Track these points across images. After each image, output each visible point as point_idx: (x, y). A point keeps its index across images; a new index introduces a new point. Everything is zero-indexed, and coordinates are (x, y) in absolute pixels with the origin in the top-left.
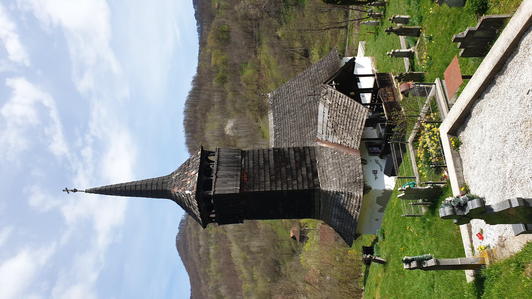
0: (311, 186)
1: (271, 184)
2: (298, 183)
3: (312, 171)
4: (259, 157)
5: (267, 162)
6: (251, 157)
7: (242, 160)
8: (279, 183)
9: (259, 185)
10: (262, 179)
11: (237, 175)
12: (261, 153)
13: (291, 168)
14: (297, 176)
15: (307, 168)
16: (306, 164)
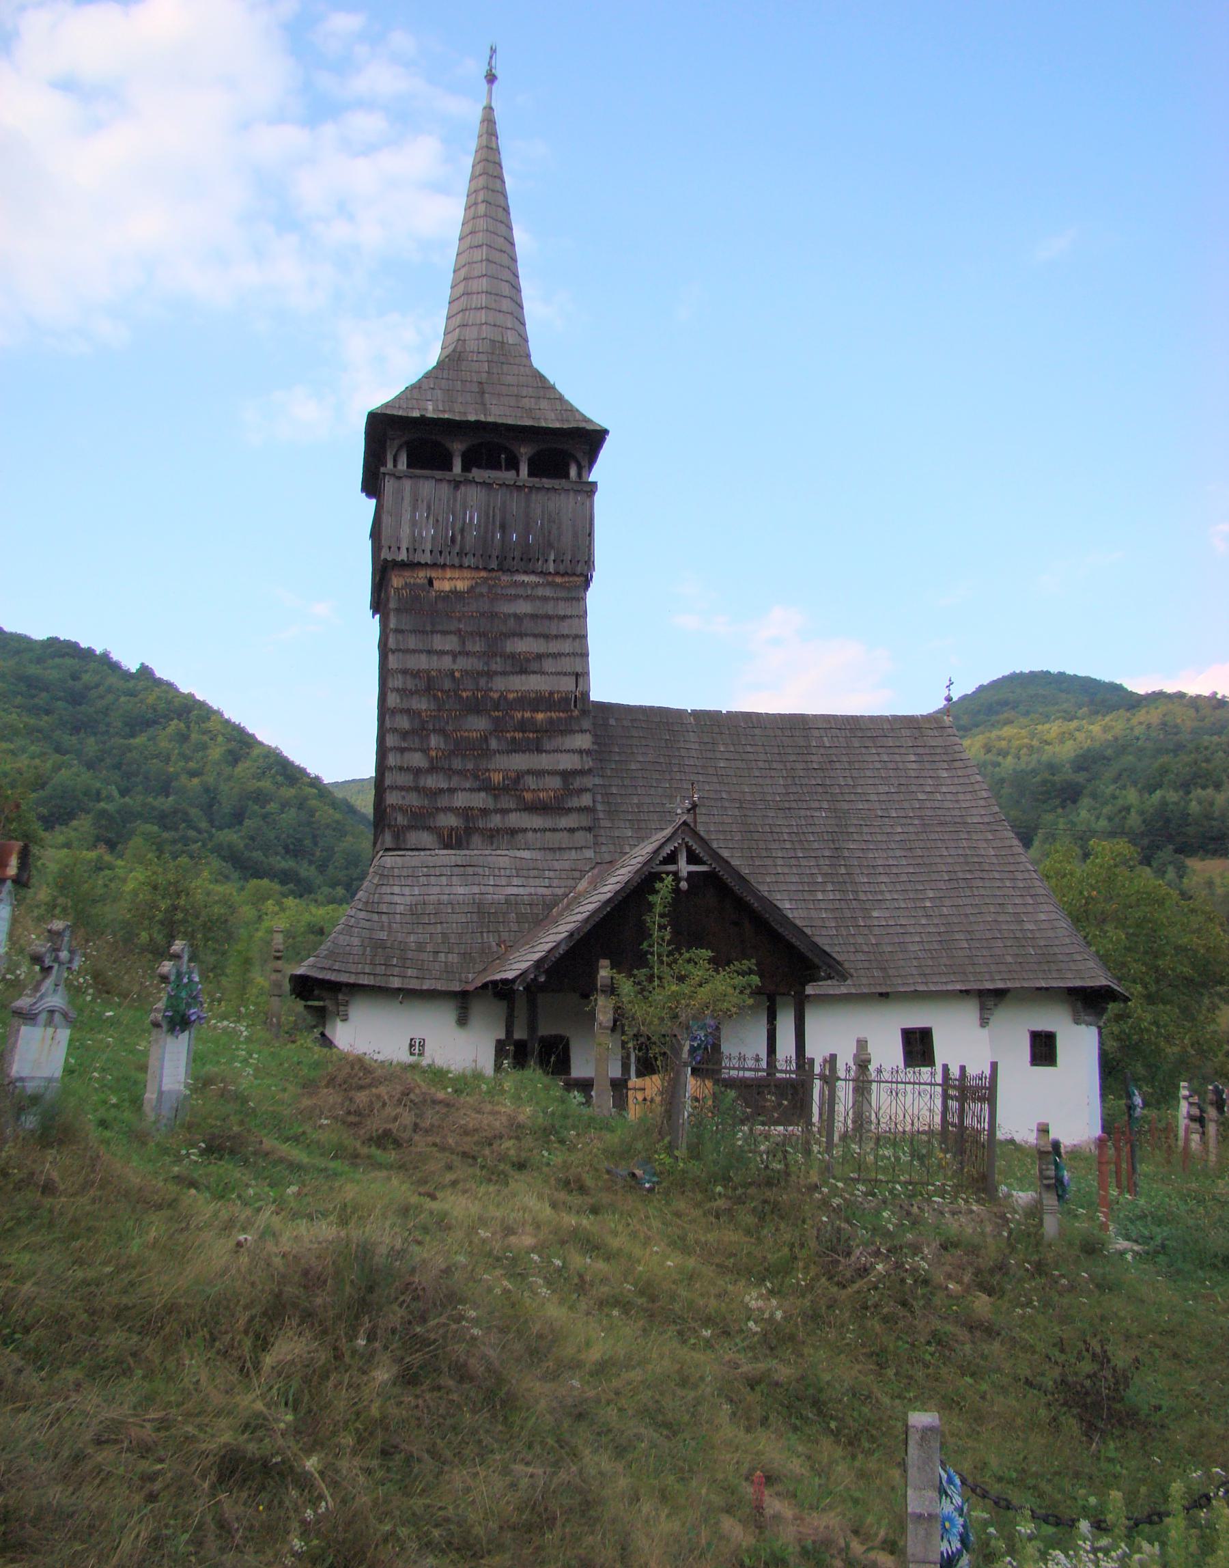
0: (401, 820)
1: (416, 674)
2: (417, 772)
3: (469, 831)
4: (546, 637)
5: (522, 665)
6: (549, 609)
7: (533, 572)
8: (421, 704)
9: (414, 631)
10: (451, 643)
11: (462, 554)
12: (566, 647)
13: (487, 753)
14: (450, 772)
15: (485, 812)
16: (504, 812)
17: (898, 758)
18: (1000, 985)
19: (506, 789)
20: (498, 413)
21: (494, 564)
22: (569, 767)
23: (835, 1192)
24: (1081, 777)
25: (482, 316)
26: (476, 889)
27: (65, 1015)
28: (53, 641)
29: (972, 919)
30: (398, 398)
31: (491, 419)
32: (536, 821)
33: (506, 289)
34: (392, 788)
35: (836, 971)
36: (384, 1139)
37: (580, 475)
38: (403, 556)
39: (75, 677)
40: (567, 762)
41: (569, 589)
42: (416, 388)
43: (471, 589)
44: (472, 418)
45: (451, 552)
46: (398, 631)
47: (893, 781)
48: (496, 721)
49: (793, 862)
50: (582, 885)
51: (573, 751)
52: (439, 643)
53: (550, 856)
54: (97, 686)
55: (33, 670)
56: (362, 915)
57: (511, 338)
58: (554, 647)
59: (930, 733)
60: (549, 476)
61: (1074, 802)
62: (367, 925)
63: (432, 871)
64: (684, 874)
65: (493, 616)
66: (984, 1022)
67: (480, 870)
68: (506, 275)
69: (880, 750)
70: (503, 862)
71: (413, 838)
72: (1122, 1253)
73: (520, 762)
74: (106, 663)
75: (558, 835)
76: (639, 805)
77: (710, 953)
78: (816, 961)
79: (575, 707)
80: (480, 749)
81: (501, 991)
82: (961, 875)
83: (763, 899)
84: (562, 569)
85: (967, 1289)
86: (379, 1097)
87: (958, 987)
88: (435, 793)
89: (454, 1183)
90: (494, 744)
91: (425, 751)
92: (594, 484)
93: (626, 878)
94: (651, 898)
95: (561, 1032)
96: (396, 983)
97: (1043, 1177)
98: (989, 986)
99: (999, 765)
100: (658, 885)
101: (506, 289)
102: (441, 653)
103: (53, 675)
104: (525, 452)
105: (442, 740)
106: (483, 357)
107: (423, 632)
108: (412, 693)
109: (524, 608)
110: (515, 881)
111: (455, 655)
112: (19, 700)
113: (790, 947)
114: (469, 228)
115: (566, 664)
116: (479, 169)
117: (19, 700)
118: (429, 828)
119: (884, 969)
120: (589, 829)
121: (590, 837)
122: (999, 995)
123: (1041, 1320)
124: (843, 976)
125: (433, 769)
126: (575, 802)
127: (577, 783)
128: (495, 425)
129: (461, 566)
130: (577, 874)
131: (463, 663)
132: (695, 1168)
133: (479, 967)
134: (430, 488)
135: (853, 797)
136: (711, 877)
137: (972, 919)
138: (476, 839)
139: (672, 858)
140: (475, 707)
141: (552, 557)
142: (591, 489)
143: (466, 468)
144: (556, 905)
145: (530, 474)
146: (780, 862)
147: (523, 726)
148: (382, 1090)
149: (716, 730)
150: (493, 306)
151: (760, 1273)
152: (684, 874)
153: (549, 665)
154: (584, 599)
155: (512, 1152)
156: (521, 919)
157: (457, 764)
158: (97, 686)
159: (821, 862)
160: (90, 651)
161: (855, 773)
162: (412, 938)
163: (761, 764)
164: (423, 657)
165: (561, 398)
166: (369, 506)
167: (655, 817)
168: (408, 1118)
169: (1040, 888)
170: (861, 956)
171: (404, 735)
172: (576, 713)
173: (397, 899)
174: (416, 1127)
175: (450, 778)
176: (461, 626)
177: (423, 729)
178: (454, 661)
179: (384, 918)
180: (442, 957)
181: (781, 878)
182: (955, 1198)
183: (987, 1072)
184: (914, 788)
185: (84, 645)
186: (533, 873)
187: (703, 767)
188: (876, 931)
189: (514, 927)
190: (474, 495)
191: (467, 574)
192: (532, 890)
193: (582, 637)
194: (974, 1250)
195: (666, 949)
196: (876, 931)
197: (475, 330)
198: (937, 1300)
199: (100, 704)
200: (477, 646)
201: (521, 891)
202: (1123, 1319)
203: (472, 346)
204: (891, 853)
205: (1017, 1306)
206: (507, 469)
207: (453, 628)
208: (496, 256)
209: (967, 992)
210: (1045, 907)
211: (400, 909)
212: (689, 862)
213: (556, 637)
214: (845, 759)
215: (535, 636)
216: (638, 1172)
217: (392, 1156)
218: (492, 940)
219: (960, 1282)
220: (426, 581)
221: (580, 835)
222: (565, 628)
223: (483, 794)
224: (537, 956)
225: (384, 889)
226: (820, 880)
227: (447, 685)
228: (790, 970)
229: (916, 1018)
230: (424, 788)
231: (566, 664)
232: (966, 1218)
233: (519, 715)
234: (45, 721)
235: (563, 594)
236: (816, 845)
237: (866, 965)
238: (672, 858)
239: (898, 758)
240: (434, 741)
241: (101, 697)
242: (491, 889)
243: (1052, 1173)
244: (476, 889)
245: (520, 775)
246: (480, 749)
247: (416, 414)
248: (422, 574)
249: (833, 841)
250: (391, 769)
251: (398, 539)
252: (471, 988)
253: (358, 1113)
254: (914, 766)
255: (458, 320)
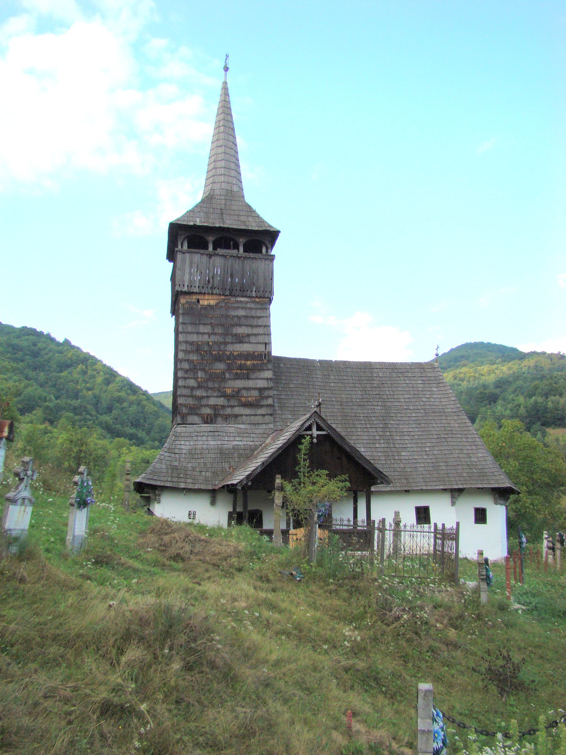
0: (185, 410)
1: (192, 343)
2: (192, 388)
3: (216, 416)
4: (252, 326)
5: (240, 339)
6: (253, 313)
7: (246, 296)
8: (194, 357)
9: (191, 324)
10: (208, 329)
12: (261, 331)
13: (224, 380)
14: (207, 389)
15: (223, 407)
16: (232, 407)
17: (413, 382)
18: (461, 487)
19: (233, 396)
20: (230, 223)
21: (227, 293)
22: (262, 386)
23: (384, 582)
24: (498, 391)
25: (222, 179)
26: (219, 443)
27: (30, 500)
28: (24, 329)
29: (448, 456)
30: (183, 216)
31: (226, 226)
32: (247, 411)
33: (233, 166)
34: (180, 396)
35: (385, 480)
36: (177, 558)
37: (267, 252)
38: (186, 289)
39: (35, 345)
40: (261, 384)
41: (262, 304)
42: (192, 211)
43: (217, 304)
44: (217, 225)
45: (208, 287)
46: (183, 323)
47: (411, 392)
48: (229, 365)
49: (365, 430)
50: (268, 441)
51: (264, 379)
52: (202, 329)
53: (253, 427)
54: (45, 349)
55: (15, 341)
56: (167, 454)
57: (235, 189)
58: (255, 331)
59: (429, 370)
60: (253, 252)
61: (495, 402)
62: (169, 459)
63: (199, 434)
64: (315, 435)
65: (227, 316)
66: (453, 504)
67: (221, 434)
68: (233, 160)
69: (405, 378)
70: (232, 430)
71: (190, 419)
72: (517, 610)
73: (240, 384)
74: (49, 338)
75: (257, 417)
76: (294, 404)
77: (327, 472)
78: (376, 475)
79: (265, 359)
80: (221, 378)
81: (231, 489)
82: (443, 436)
83: (351, 447)
84: (259, 295)
85: (446, 627)
86: (174, 538)
87: (441, 487)
88: (201, 398)
89: (209, 578)
90: (227, 375)
91: (196, 379)
92: (274, 256)
93: (288, 437)
94: (300, 446)
95: (258, 508)
96: (182, 486)
97: (480, 575)
98: (456, 487)
99: (460, 385)
100: (303, 441)
101: (233, 166)
102: (203, 334)
103: (24, 344)
104: (242, 241)
105: (203, 374)
106: (223, 197)
107: (195, 324)
108: (190, 352)
109: (241, 313)
110: (237, 439)
111: (209, 335)
112: (9, 355)
113: (364, 468)
114: (216, 138)
115: (261, 339)
116: (221, 111)
117: (9, 355)
118: (197, 414)
119: (407, 479)
120: (271, 415)
121: (271, 418)
122: (460, 491)
123: (479, 641)
124: (388, 482)
125: (199, 387)
126: (265, 402)
127: (266, 393)
128: (228, 228)
129: (212, 294)
130: (266, 436)
131: (213, 338)
132: (320, 571)
133: (221, 478)
134: (198, 258)
135: (393, 400)
136: (328, 436)
137: (448, 456)
138: (219, 419)
139: (309, 428)
140: (219, 359)
141: (254, 290)
142: (272, 258)
143: (215, 248)
144: (256, 449)
145: (244, 251)
146: (359, 430)
147: (241, 367)
148: (176, 535)
149: (330, 369)
150: (227, 173)
151: (350, 619)
152: (315, 435)
153: (253, 339)
154: (269, 309)
155: (236, 564)
156: (240, 456)
157: (210, 384)
158: (45, 349)
159: (378, 430)
160: (41, 334)
161: (394, 389)
162: (190, 465)
163: (350, 385)
164: (195, 336)
165: (258, 216)
166: (170, 266)
167: (302, 409)
168: (188, 548)
169: (479, 442)
170: (396, 473)
171: (186, 371)
172: (265, 361)
173: (183, 447)
174: (192, 552)
175: (207, 391)
176: (213, 321)
177: (195, 369)
178: (209, 337)
179: (177, 456)
180: (203, 474)
181: (360, 437)
182: (440, 584)
183: (455, 527)
184: (421, 396)
185: (39, 330)
186: (245, 435)
187: (324, 386)
188: (404, 461)
189: (237, 460)
190: (218, 261)
191: (215, 297)
192: (245, 443)
193: (268, 326)
194: (449, 608)
195: (307, 470)
196: (404, 461)
197: (219, 184)
198: (431, 632)
199: (46, 357)
200: (220, 330)
201: (240, 443)
202: (517, 640)
203: (217, 192)
204: (410, 426)
205: (468, 634)
206: (234, 249)
207: (209, 322)
208: (228, 151)
209: (445, 490)
210: (481, 451)
211: (184, 451)
212: (317, 430)
213: (256, 326)
214: (389, 382)
215: (246, 326)
216: (294, 573)
217: (181, 565)
218: (226, 466)
219: (442, 623)
220: (196, 301)
221: (267, 417)
222: (260, 322)
223: (222, 399)
224: (247, 473)
225: (177, 442)
226: (378, 438)
227: (206, 348)
228: (364, 479)
229: (422, 502)
230: (195, 396)
231: (261, 339)
232: (445, 594)
233: (239, 362)
234: (21, 365)
235: (259, 306)
236: (376, 422)
237: (399, 477)
238: (309, 428)
239: (413, 382)
240: (200, 374)
241: (47, 354)
242: (226, 442)
243: (484, 573)
244: (219, 443)
245: (239, 390)
246: (221, 378)
247: (192, 224)
248: (194, 297)
249: (384, 420)
250: (180, 387)
251: (183, 281)
252: (217, 488)
253: (165, 545)
254: (421, 386)
255: (211, 180)
